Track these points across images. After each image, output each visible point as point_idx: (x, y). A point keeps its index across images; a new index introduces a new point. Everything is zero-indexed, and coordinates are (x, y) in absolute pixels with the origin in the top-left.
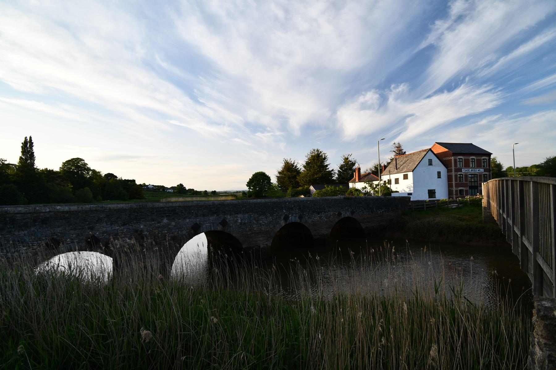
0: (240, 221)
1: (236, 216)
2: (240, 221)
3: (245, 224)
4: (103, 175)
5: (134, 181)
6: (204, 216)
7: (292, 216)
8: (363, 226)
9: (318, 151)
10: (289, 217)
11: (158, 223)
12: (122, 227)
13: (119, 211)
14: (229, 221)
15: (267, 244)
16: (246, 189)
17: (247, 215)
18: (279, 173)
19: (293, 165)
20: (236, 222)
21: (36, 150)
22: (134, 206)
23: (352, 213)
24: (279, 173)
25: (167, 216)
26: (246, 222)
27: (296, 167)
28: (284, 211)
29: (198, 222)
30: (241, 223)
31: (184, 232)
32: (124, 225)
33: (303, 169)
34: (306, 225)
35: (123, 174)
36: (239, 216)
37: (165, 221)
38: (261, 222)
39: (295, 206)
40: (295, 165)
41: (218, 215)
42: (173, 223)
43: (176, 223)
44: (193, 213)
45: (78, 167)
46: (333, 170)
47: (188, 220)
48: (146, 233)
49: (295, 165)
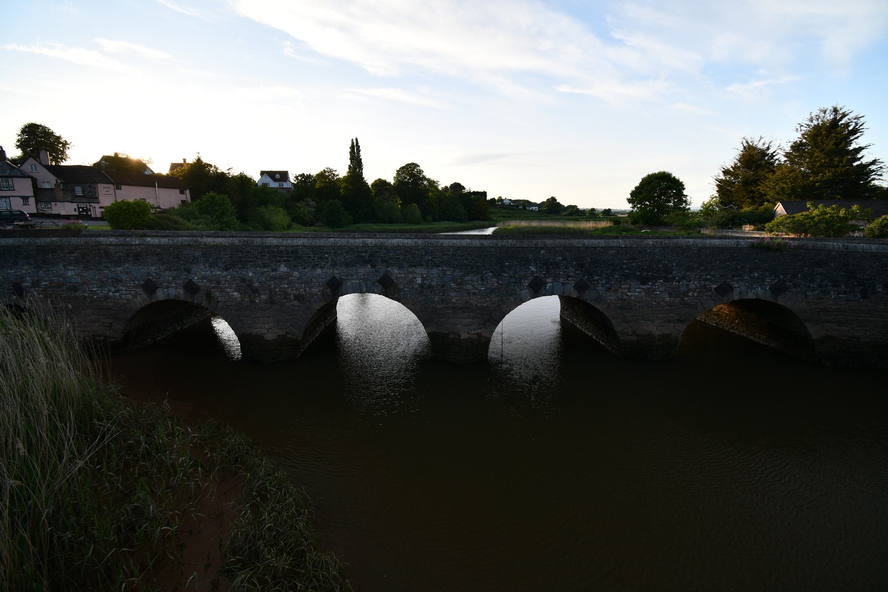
0: (419, 281)
1: (411, 270)
2: (419, 281)
3: (430, 287)
4: (440, 188)
5: (484, 194)
6: (347, 265)
7: (554, 280)
8: (814, 331)
9: (835, 110)
10: (545, 283)
11: (274, 270)
12: (225, 273)
13: (217, 247)
14: (397, 278)
15: (479, 335)
16: (628, 207)
17: (435, 271)
18: (726, 172)
19: (763, 153)
20: (412, 281)
21: (363, 155)
22: (236, 241)
23: (777, 290)
24: (726, 172)
25: (285, 261)
26: (434, 283)
27: (772, 156)
28: (533, 269)
29: (338, 276)
30: (422, 286)
31: (315, 290)
32: (226, 269)
33: (783, 159)
34: (599, 307)
35: (471, 185)
36: (417, 270)
37: (283, 269)
38: (469, 287)
39: (565, 259)
40: (770, 151)
41: (373, 266)
42: (296, 274)
43: (300, 273)
44: (327, 258)
45: (412, 175)
46: (874, 162)
47: (319, 271)
48: (256, 285)
49: (770, 151)
